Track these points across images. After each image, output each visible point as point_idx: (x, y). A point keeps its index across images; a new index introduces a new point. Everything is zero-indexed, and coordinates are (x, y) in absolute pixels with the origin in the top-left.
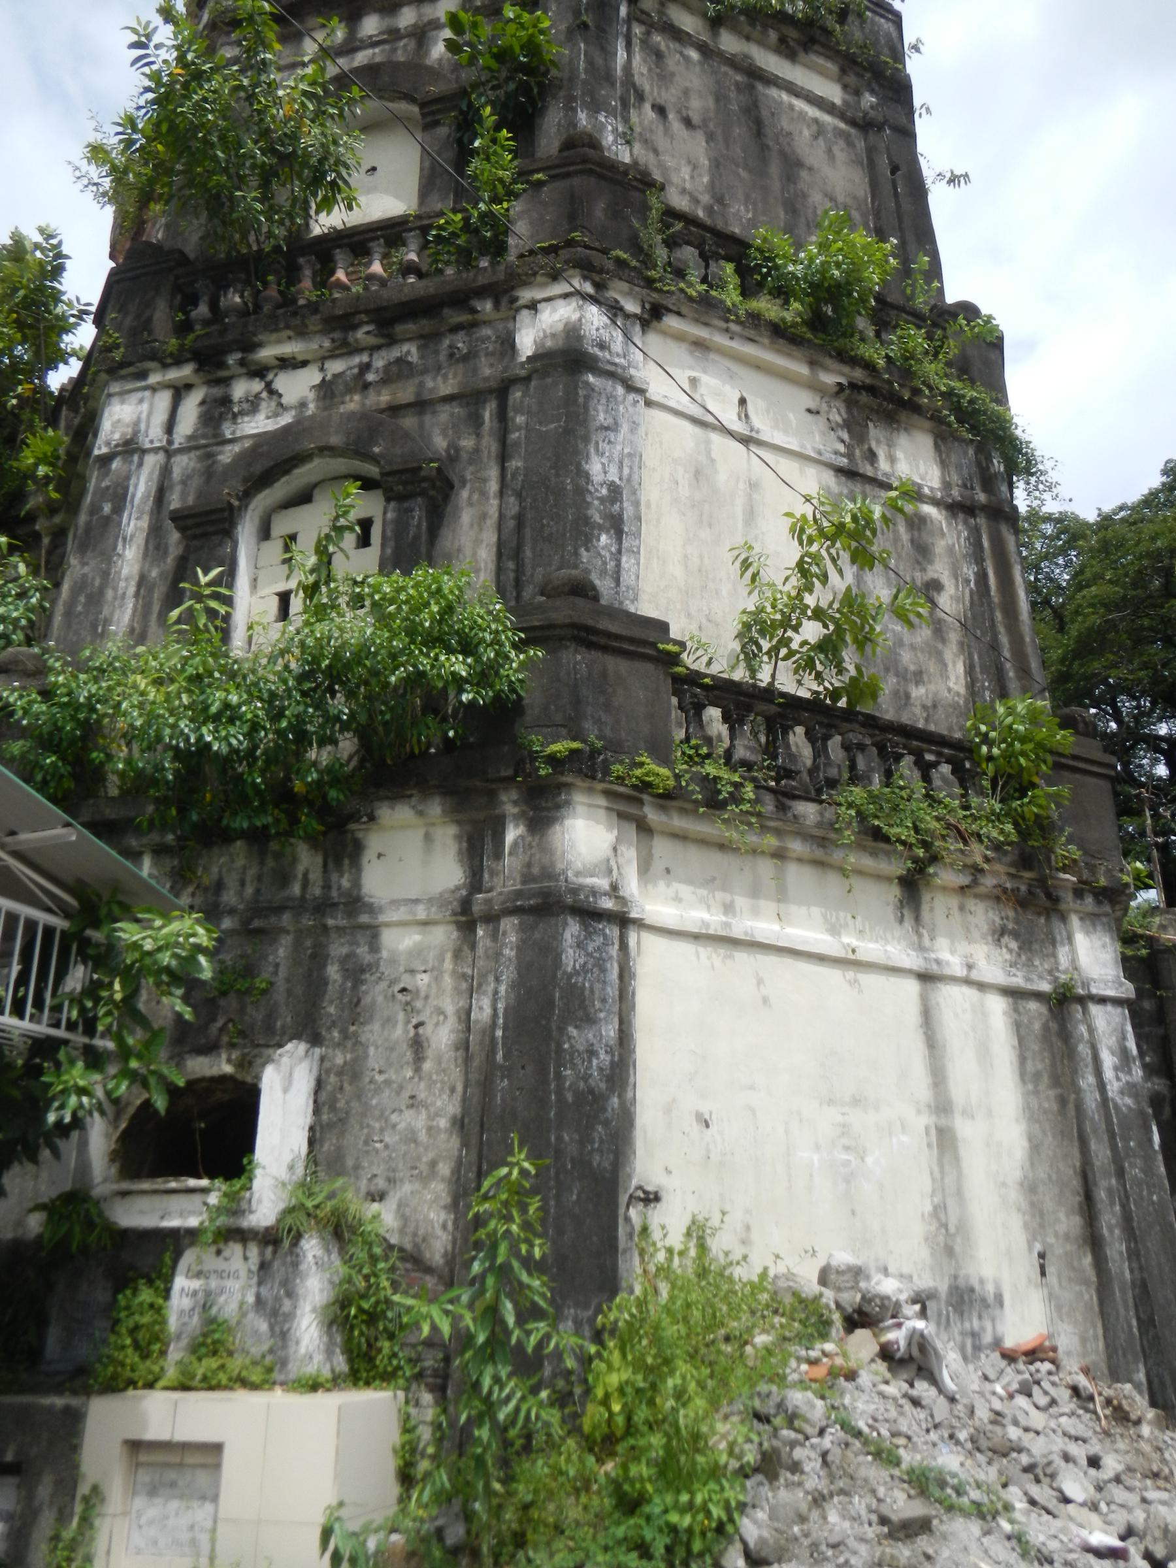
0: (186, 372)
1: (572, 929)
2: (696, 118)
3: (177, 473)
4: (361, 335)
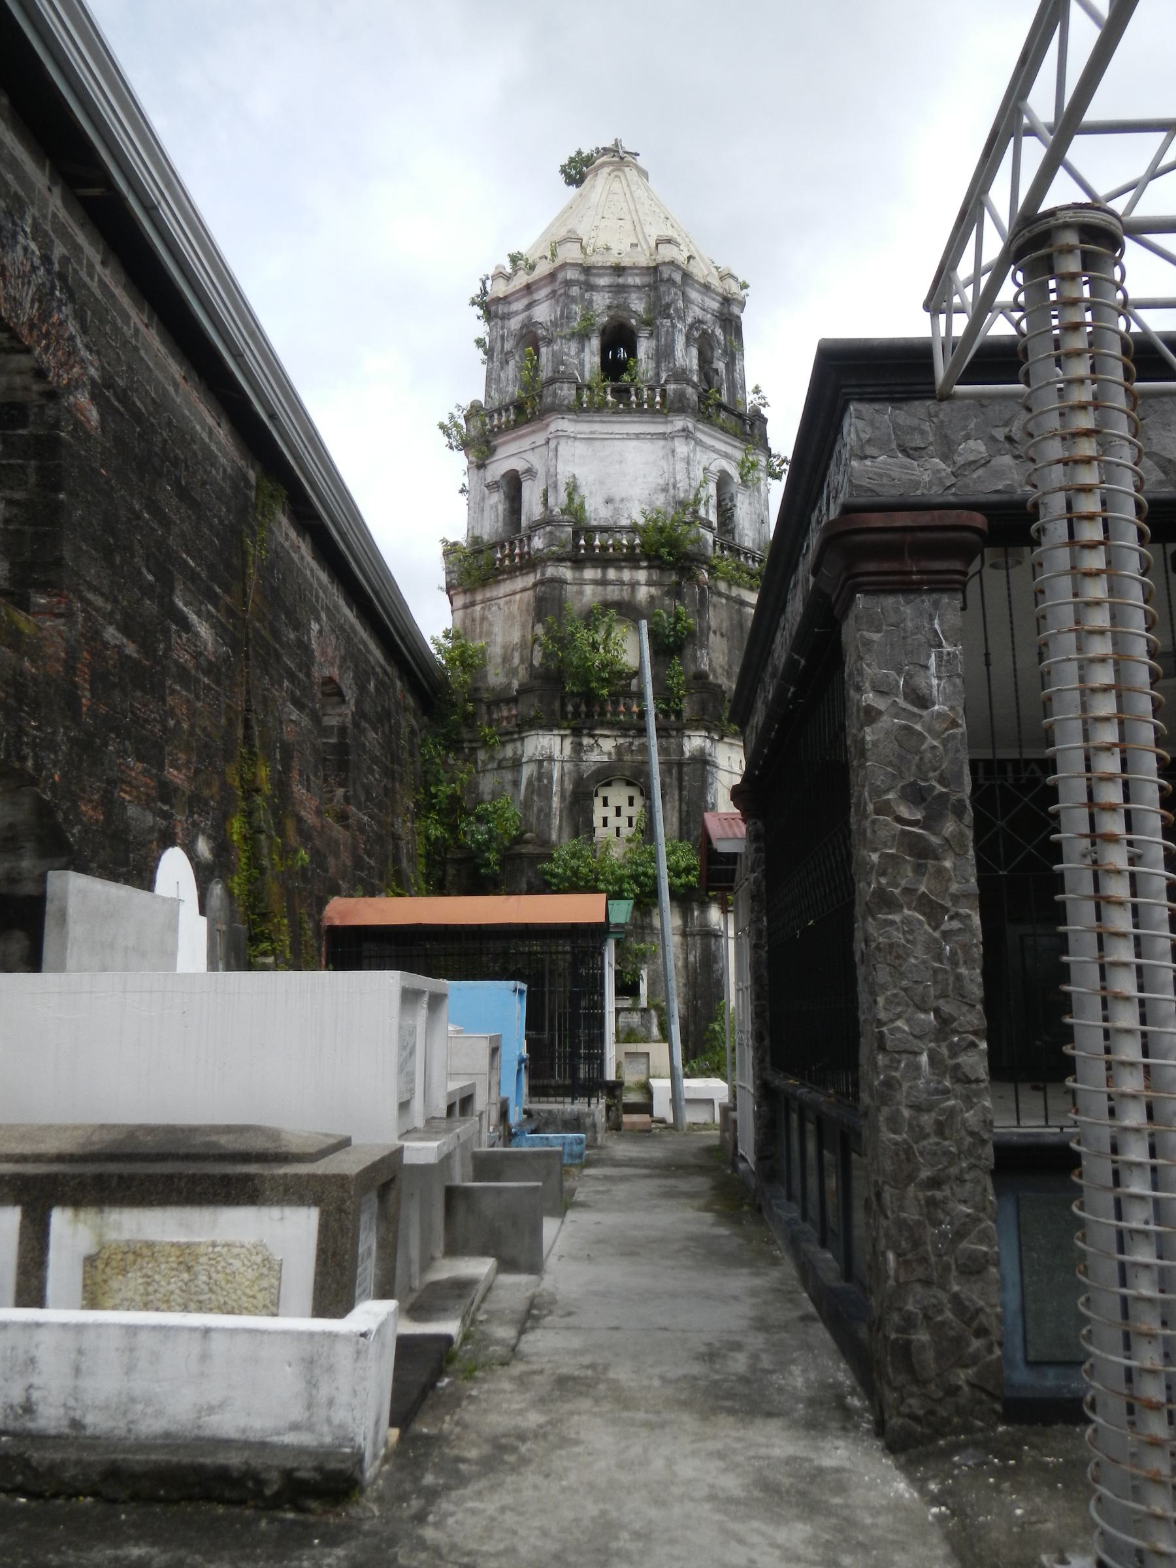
0: (568, 732)
1: (713, 940)
2: (724, 631)
3: (566, 769)
4: (631, 733)
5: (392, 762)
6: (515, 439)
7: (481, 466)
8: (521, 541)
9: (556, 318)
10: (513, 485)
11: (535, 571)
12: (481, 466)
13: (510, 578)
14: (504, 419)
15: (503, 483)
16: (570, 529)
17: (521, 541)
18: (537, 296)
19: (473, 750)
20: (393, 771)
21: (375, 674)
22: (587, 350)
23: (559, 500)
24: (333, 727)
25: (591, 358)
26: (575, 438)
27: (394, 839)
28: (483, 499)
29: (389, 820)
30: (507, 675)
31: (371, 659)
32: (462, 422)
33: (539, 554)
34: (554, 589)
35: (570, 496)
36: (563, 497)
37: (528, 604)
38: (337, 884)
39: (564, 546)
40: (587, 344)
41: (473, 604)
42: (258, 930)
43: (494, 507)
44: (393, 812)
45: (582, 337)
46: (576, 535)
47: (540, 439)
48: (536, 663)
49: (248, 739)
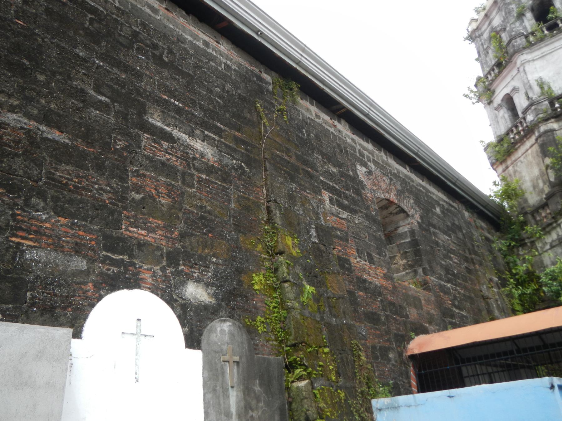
5: (470, 254)
6: (502, 81)
7: (490, 103)
8: (521, 123)
9: (504, 17)
10: (509, 101)
11: (534, 133)
12: (490, 103)
13: (522, 144)
14: (493, 75)
15: (504, 104)
16: (547, 102)
17: (521, 123)
18: (491, 17)
19: (533, 243)
20: (472, 259)
21: (439, 205)
22: (525, 21)
23: (535, 93)
24: (406, 232)
25: (529, 22)
26: (533, 60)
27: (484, 299)
28: (496, 117)
29: (477, 287)
30: (539, 195)
31: (434, 197)
32: (475, 89)
33: (533, 122)
34: (549, 136)
35: (542, 88)
36: (537, 89)
37: (537, 151)
38: (422, 326)
39: (546, 112)
40: (524, 18)
41: (507, 167)
42: (291, 359)
43: (503, 117)
44: (479, 282)
45: (521, 16)
46: (552, 104)
47: (514, 72)
48: (552, 179)
49: (270, 220)
